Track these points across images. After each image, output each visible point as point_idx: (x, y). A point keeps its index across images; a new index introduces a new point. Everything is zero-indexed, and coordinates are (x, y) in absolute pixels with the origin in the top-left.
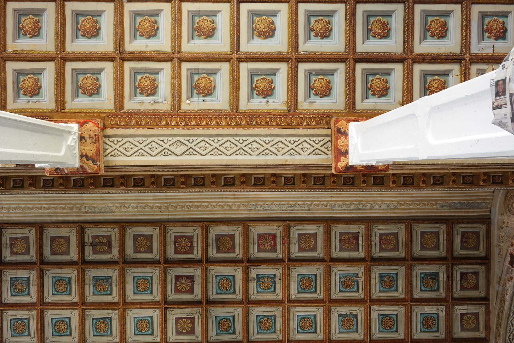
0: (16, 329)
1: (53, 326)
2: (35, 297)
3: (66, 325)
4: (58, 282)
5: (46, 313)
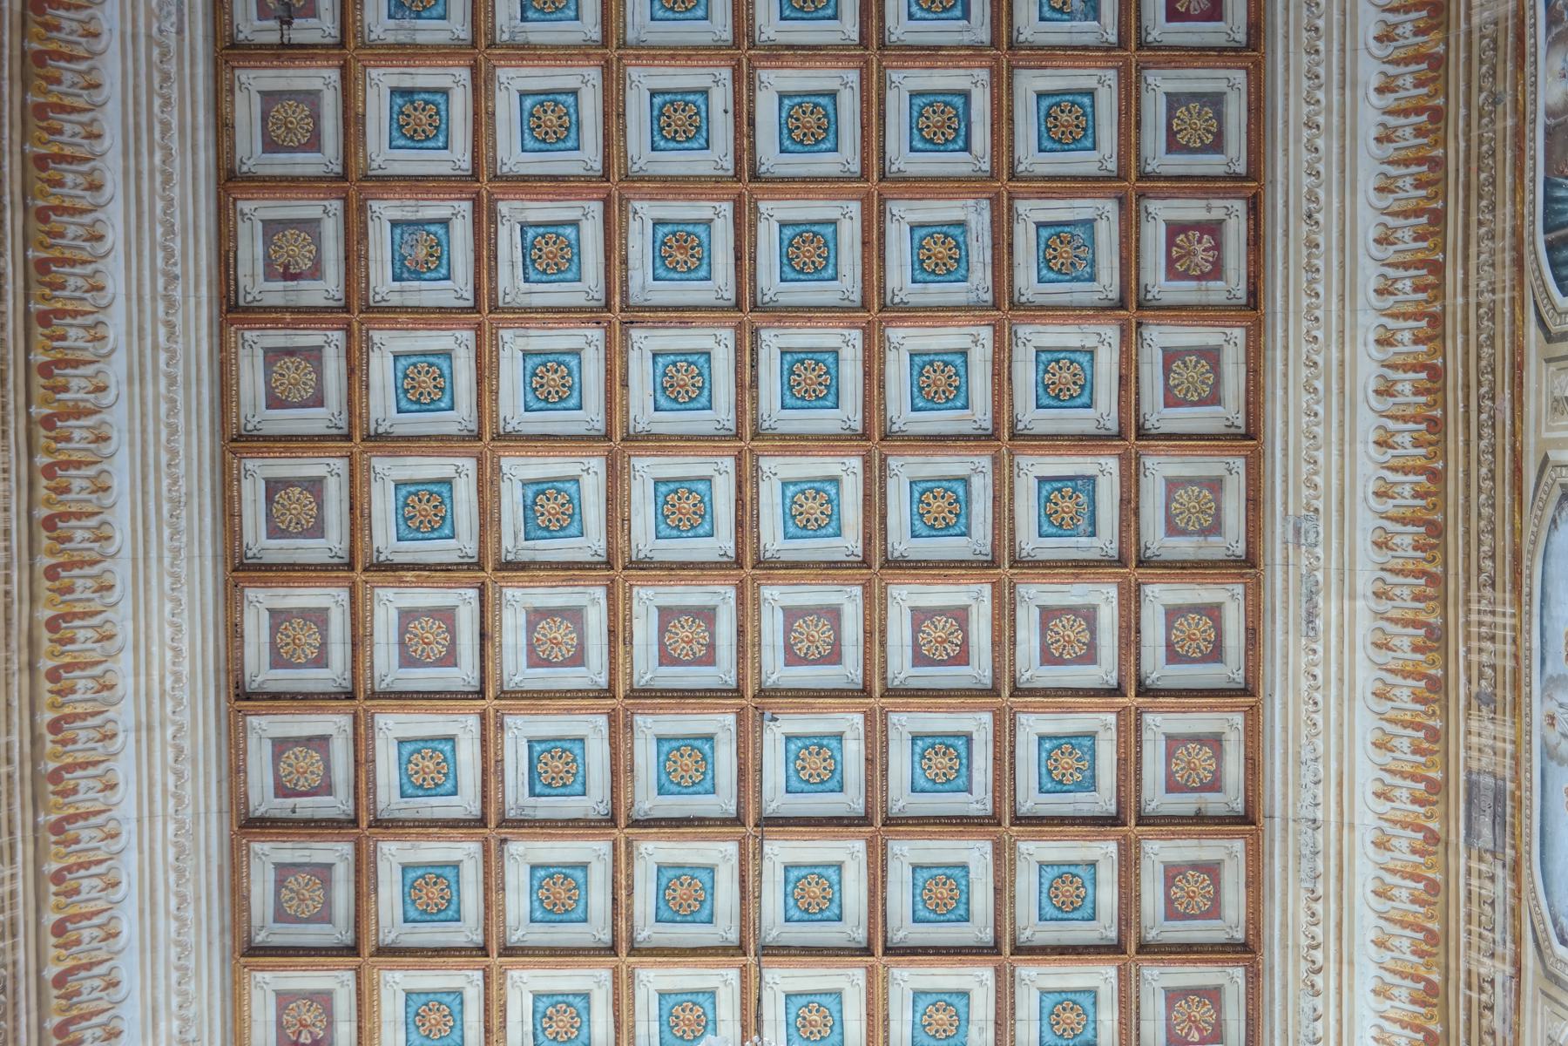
0: (556, 264)
1: (548, 147)
2: (456, 204)
3: (542, 106)
4: (407, 131)
5: (505, 169)
